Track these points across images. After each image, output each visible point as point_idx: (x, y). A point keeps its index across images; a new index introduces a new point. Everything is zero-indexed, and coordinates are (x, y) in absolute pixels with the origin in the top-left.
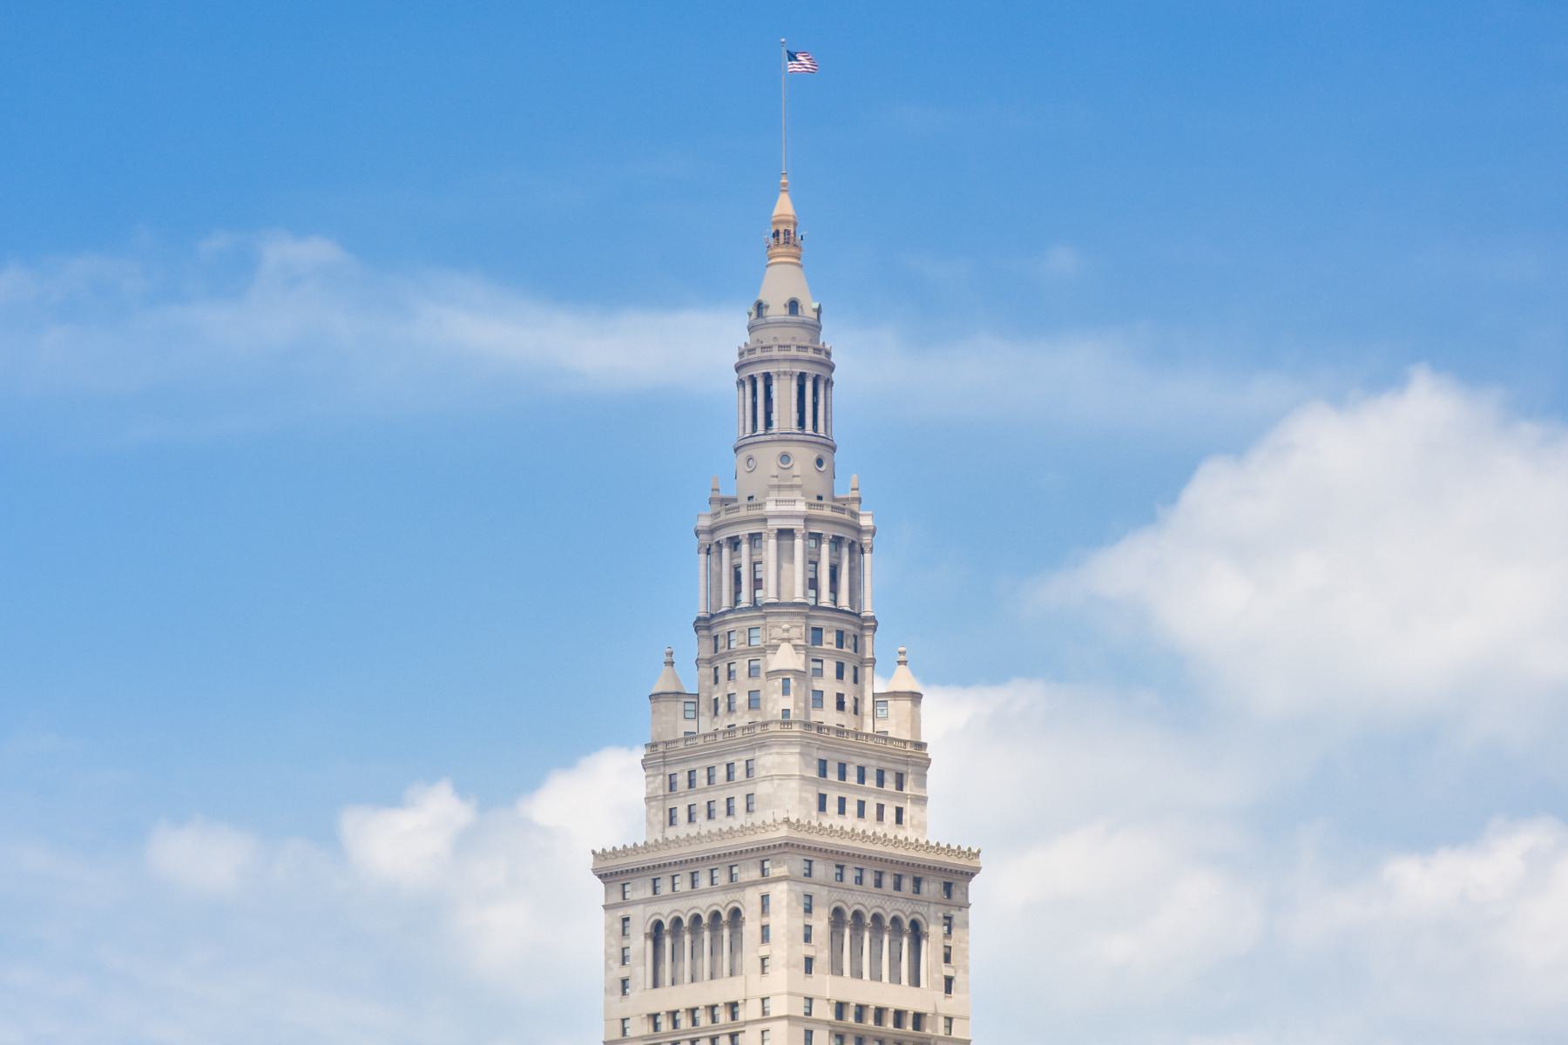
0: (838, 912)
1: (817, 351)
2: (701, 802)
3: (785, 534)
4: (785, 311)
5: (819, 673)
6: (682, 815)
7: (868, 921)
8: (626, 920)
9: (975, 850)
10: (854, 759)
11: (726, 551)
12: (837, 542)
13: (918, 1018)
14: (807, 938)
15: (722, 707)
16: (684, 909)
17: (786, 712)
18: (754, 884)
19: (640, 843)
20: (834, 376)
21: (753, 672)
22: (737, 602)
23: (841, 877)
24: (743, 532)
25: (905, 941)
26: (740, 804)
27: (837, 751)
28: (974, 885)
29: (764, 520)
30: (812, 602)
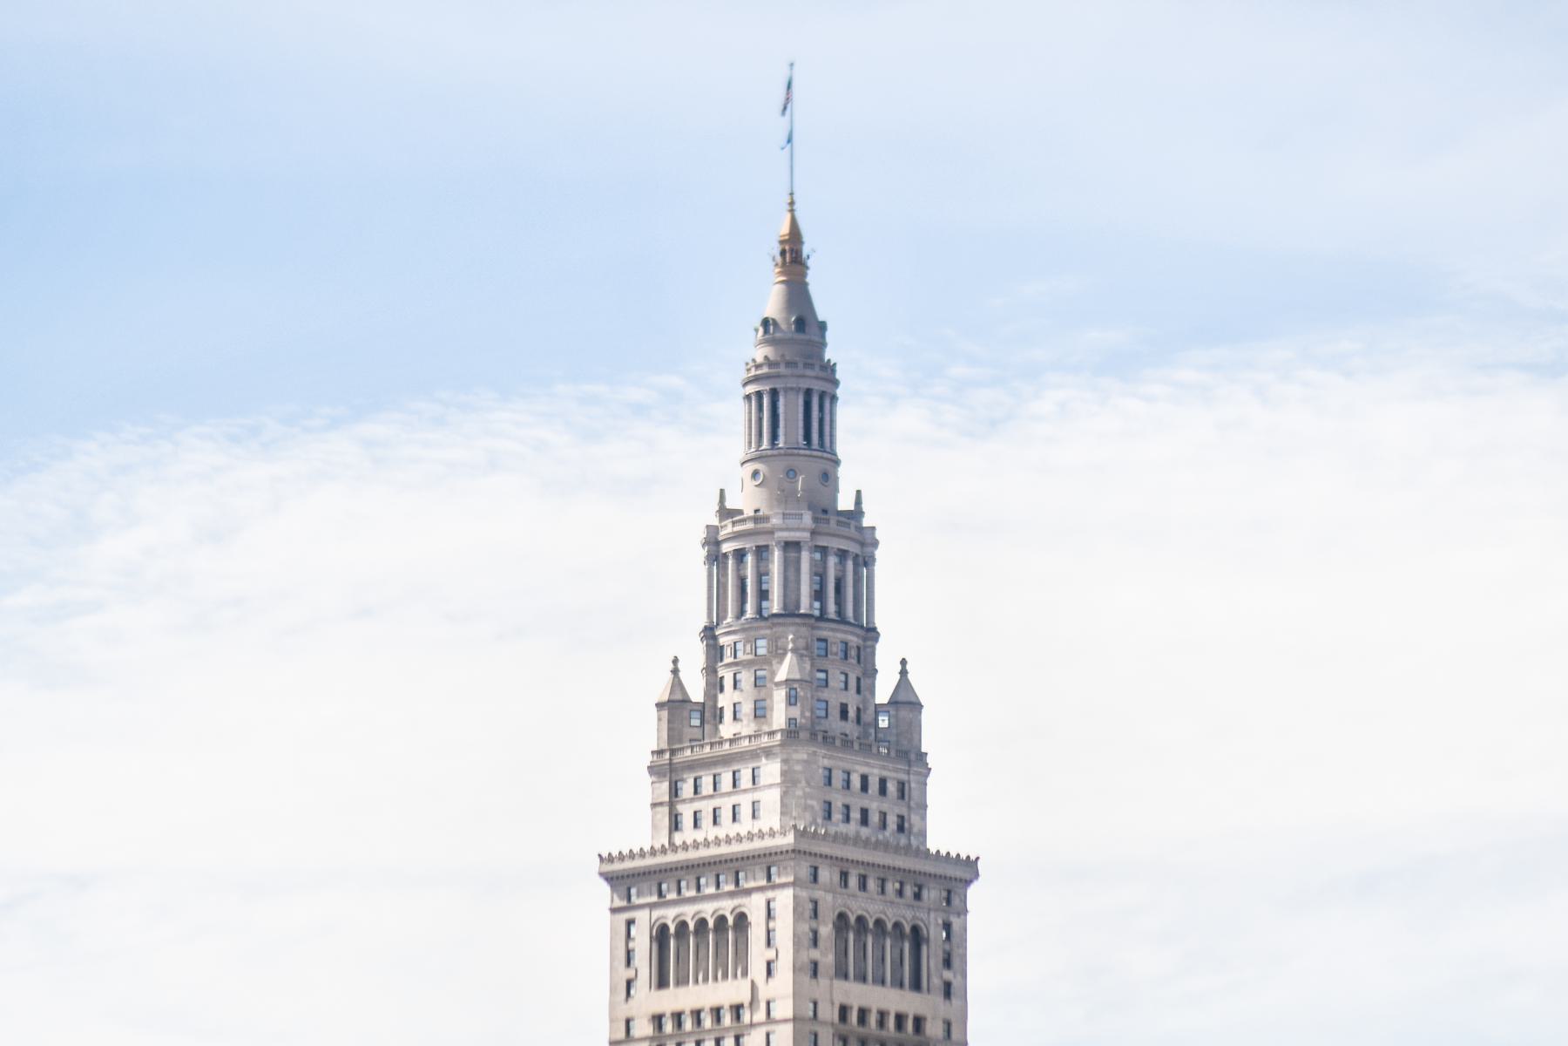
0: (842, 917)
2: (706, 807)
3: (791, 546)
7: (871, 925)
8: (630, 923)
9: (973, 858)
10: (857, 767)
11: (730, 562)
14: (815, 942)
20: (839, 392)
26: (745, 812)
28: (973, 892)
29: (771, 532)
30: (817, 613)
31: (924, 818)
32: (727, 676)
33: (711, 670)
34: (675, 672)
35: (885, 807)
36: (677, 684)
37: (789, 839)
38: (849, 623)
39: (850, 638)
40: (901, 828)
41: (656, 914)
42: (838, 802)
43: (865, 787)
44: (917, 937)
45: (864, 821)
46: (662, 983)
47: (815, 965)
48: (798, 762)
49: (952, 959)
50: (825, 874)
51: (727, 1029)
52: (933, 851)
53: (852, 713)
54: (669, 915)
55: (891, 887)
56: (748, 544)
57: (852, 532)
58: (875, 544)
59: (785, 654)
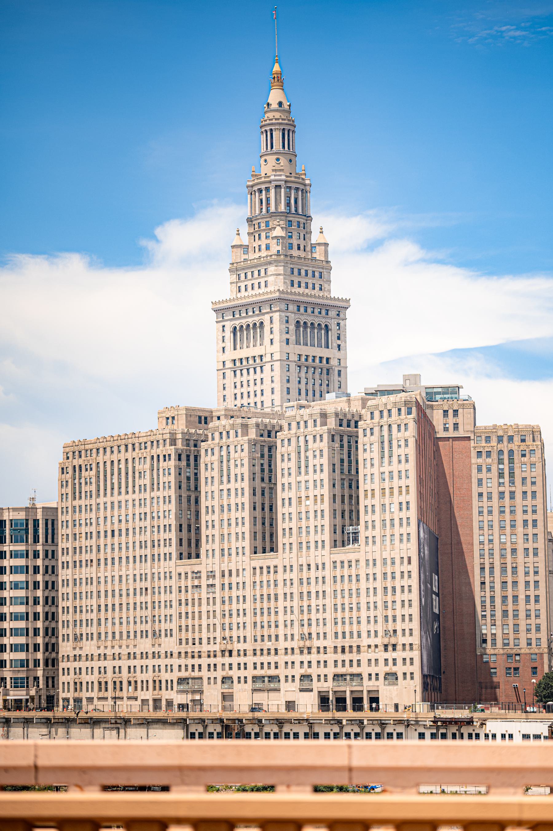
0: (298, 322)
1: (289, 120)
2: (249, 284)
3: (278, 187)
4: (277, 106)
5: (291, 237)
6: (243, 289)
8: (224, 326)
9: (348, 299)
11: (257, 194)
12: (297, 189)
15: (257, 250)
17: (278, 251)
18: (267, 313)
21: (267, 237)
23: (299, 310)
24: (263, 187)
25: (323, 332)
26: (263, 284)
27: (297, 264)
28: (348, 311)
29: (270, 182)
30: (288, 211)
31: (329, 285)
35: (314, 282)
37: (277, 294)
39: (301, 220)
40: (321, 289)
43: (307, 275)
47: (288, 340)
50: (291, 307)
52: (332, 297)
53: (302, 248)
54: (237, 323)
55: (317, 311)
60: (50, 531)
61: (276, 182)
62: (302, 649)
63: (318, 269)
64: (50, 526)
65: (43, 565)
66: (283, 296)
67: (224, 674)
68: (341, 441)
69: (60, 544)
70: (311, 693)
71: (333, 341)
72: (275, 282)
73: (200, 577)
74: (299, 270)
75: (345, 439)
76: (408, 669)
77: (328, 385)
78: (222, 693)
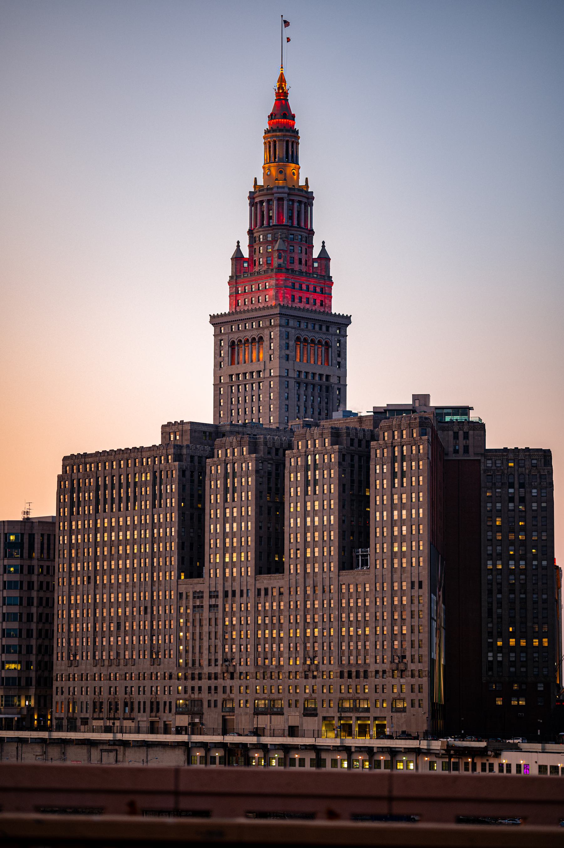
0: (298, 339)
3: (280, 200)
9: (349, 315)
12: (300, 202)
13: (328, 377)
14: (288, 348)
16: (242, 336)
19: (227, 312)
22: (263, 224)
28: (349, 329)
31: (330, 301)
32: (256, 247)
33: (251, 246)
34: (238, 246)
36: (238, 250)
38: (303, 228)
40: (321, 305)
41: (231, 336)
42: (297, 295)
44: (327, 345)
45: (308, 303)
46: (232, 363)
47: (288, 355)
48: (282, 280)
49: (342, 353)
50: (291, 323)
51: (255, 379)
52: (333, 313)
53: (303, 262)
54: (235, 337)
56: (265, 198)
57: (304, 194)
58: (313, 198)
59: (277, 240)
60: (45, 546)
61: (278, 195)
62: (307, 673)
63: (319, 285)
64: (46, 541)
65: (38, 581)
66: (284, 311)
67: (225, 696)
68: (352, 460)
69: (57, 559)
70: (316, 718)
71: (333, 358)
72: (276, 296)
73: (202, 597)
74: (301, 285)
75: (356, 458)
76: (416, 696)
77: (327, 403)
78: (223, 716)
